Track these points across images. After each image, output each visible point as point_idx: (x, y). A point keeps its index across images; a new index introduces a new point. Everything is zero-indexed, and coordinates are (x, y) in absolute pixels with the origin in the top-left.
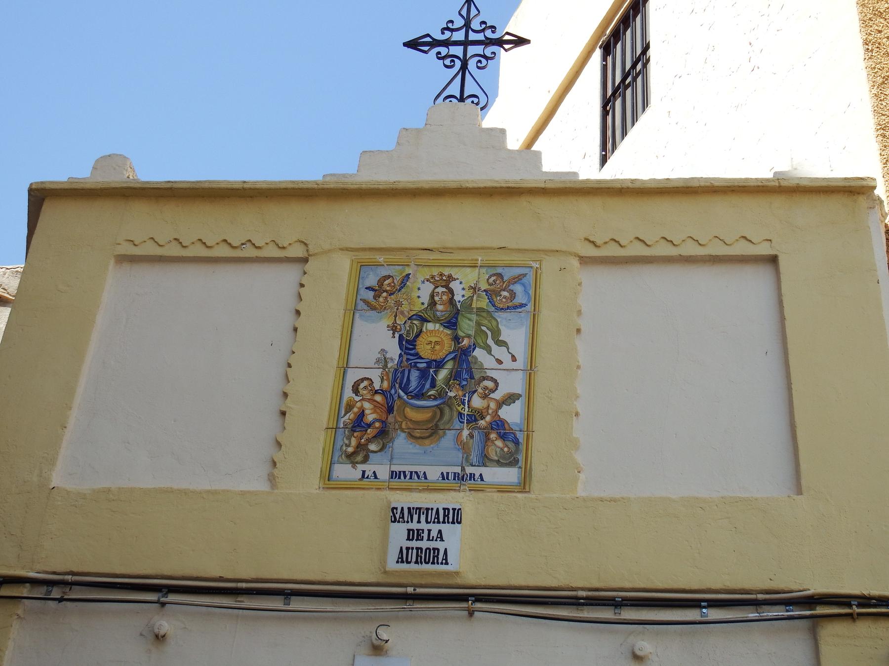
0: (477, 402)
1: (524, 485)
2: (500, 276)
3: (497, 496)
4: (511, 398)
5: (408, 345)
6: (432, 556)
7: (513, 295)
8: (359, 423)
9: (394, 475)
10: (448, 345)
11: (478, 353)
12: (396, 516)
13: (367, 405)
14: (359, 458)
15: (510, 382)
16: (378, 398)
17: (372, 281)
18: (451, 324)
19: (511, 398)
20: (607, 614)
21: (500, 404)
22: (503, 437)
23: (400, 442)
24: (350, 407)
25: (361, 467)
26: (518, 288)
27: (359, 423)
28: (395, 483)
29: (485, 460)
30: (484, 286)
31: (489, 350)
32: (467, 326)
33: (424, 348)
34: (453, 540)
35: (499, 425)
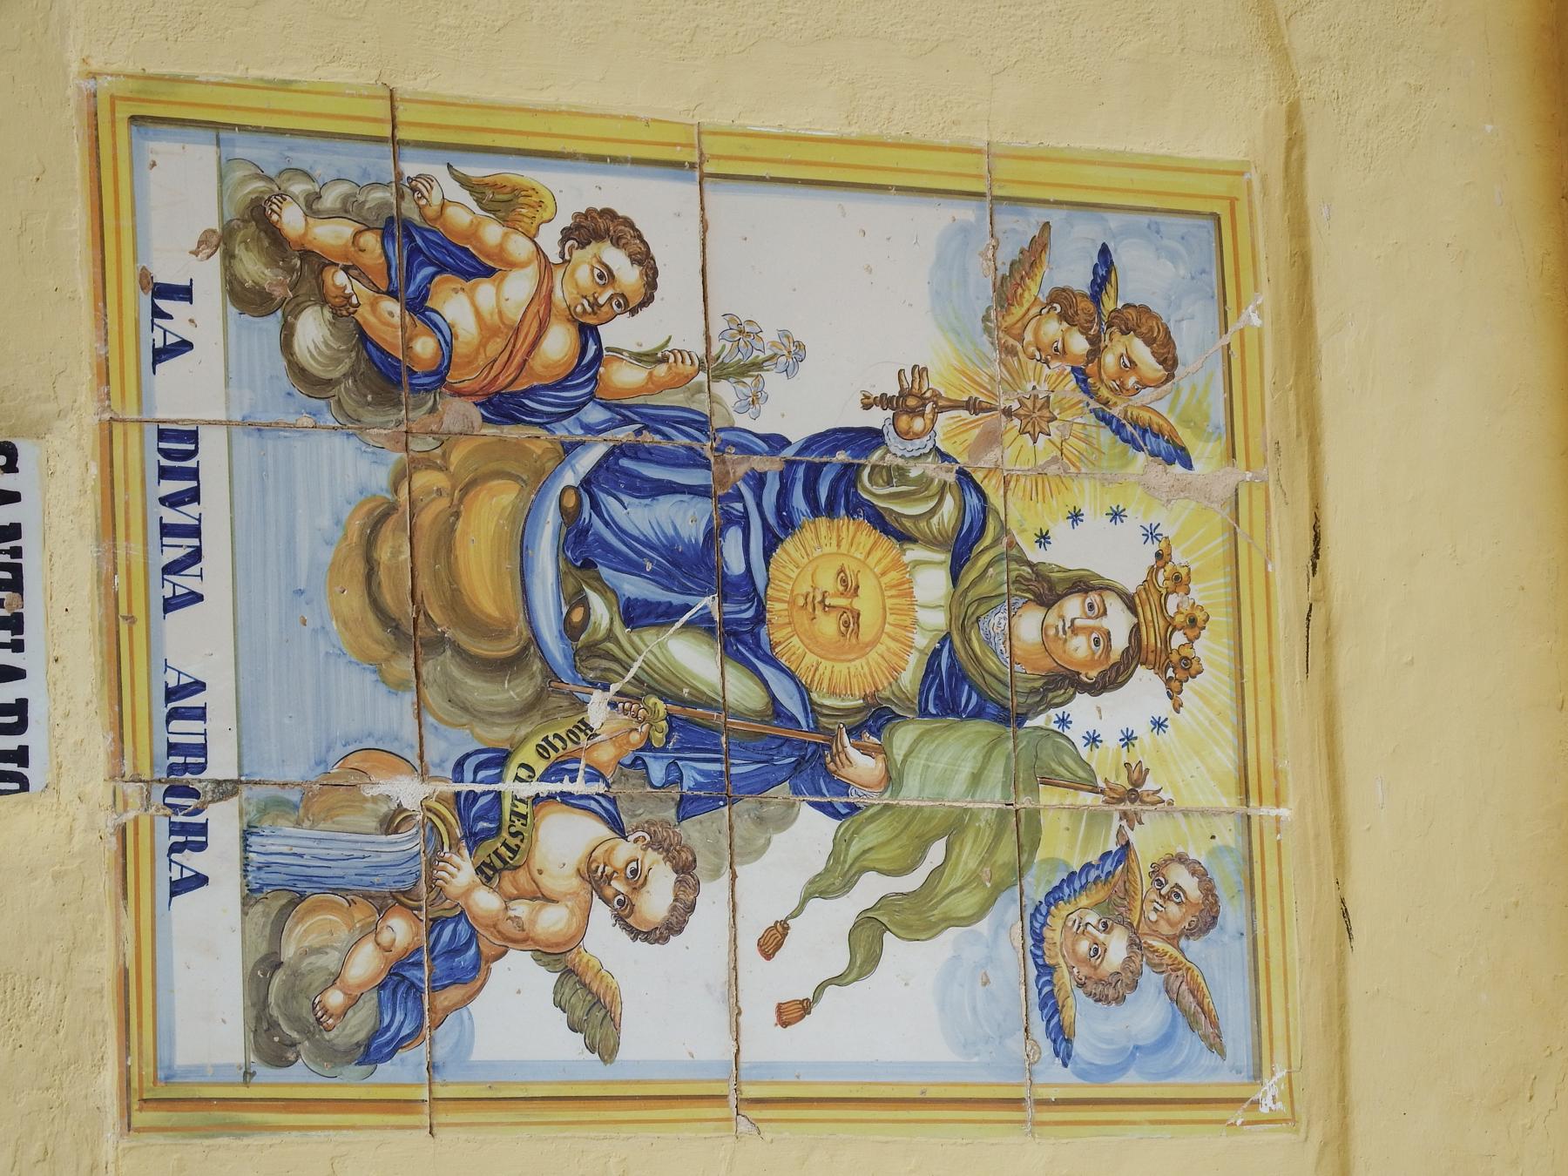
0: (564, 840)
1: (161, 1099)
2: (1207, 919)
3: (101, 966)
4: (592, 1009)
5: (832, 477)
7: (1111, 990)
8: (427, 256)
9: (178, 447)
10: (842, 678)
11: (809, 834)
13: (518, 288)
14: (254, 268)
15: (670, 1002)
16: (558, 345)
17: (1144, 277)
18: (950, 689)
19: (592, 1009)
21: (559, 957)
22: (398, 980)
23: (344, 467)
24: (503, 202)
25: (207, 277)
26: (1147, 1011)
27: (427, 256)
28: (140, 455)
29: (277, 895)
30: (1149, 842)
31: (823, 887)
32: (944, 765)
33: (821, 555)
35: (451, 958)
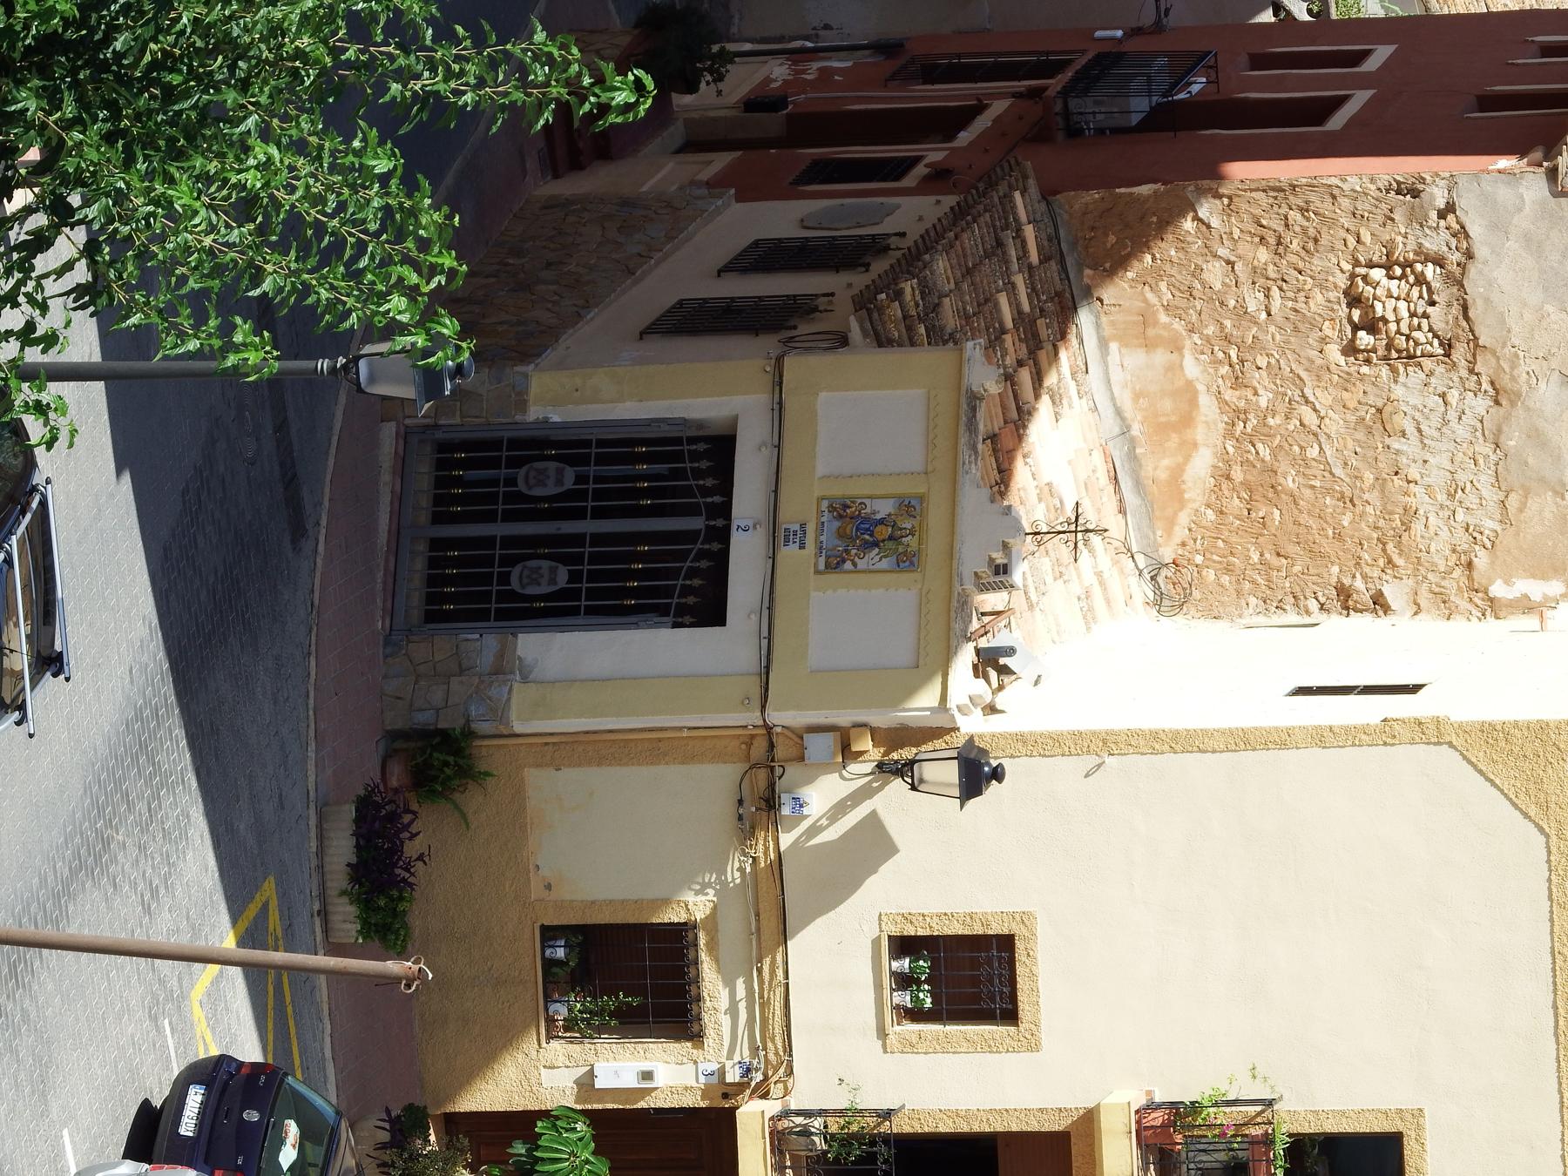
1: (817, 572)
4: (855, 565)
5: (882, 522)
6: (787, 541)
8: (846, 507)
12: (803, 526)
15: (861, 564)
19: (855, 565)
20: (766, 604)
23: (837, 524)
27: (846, 507)
29: (828, 557)
32: (890, 544)
33: (879, 528)
34: (793, 548)
35: (844, 561)
